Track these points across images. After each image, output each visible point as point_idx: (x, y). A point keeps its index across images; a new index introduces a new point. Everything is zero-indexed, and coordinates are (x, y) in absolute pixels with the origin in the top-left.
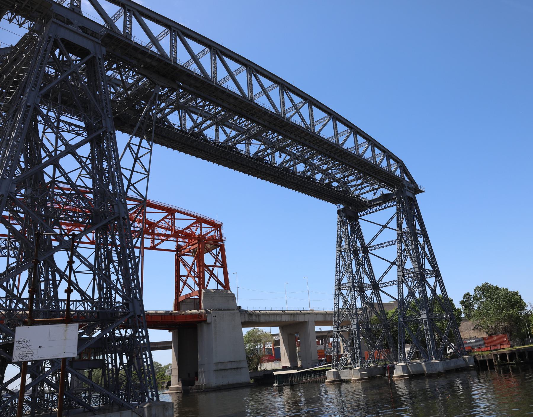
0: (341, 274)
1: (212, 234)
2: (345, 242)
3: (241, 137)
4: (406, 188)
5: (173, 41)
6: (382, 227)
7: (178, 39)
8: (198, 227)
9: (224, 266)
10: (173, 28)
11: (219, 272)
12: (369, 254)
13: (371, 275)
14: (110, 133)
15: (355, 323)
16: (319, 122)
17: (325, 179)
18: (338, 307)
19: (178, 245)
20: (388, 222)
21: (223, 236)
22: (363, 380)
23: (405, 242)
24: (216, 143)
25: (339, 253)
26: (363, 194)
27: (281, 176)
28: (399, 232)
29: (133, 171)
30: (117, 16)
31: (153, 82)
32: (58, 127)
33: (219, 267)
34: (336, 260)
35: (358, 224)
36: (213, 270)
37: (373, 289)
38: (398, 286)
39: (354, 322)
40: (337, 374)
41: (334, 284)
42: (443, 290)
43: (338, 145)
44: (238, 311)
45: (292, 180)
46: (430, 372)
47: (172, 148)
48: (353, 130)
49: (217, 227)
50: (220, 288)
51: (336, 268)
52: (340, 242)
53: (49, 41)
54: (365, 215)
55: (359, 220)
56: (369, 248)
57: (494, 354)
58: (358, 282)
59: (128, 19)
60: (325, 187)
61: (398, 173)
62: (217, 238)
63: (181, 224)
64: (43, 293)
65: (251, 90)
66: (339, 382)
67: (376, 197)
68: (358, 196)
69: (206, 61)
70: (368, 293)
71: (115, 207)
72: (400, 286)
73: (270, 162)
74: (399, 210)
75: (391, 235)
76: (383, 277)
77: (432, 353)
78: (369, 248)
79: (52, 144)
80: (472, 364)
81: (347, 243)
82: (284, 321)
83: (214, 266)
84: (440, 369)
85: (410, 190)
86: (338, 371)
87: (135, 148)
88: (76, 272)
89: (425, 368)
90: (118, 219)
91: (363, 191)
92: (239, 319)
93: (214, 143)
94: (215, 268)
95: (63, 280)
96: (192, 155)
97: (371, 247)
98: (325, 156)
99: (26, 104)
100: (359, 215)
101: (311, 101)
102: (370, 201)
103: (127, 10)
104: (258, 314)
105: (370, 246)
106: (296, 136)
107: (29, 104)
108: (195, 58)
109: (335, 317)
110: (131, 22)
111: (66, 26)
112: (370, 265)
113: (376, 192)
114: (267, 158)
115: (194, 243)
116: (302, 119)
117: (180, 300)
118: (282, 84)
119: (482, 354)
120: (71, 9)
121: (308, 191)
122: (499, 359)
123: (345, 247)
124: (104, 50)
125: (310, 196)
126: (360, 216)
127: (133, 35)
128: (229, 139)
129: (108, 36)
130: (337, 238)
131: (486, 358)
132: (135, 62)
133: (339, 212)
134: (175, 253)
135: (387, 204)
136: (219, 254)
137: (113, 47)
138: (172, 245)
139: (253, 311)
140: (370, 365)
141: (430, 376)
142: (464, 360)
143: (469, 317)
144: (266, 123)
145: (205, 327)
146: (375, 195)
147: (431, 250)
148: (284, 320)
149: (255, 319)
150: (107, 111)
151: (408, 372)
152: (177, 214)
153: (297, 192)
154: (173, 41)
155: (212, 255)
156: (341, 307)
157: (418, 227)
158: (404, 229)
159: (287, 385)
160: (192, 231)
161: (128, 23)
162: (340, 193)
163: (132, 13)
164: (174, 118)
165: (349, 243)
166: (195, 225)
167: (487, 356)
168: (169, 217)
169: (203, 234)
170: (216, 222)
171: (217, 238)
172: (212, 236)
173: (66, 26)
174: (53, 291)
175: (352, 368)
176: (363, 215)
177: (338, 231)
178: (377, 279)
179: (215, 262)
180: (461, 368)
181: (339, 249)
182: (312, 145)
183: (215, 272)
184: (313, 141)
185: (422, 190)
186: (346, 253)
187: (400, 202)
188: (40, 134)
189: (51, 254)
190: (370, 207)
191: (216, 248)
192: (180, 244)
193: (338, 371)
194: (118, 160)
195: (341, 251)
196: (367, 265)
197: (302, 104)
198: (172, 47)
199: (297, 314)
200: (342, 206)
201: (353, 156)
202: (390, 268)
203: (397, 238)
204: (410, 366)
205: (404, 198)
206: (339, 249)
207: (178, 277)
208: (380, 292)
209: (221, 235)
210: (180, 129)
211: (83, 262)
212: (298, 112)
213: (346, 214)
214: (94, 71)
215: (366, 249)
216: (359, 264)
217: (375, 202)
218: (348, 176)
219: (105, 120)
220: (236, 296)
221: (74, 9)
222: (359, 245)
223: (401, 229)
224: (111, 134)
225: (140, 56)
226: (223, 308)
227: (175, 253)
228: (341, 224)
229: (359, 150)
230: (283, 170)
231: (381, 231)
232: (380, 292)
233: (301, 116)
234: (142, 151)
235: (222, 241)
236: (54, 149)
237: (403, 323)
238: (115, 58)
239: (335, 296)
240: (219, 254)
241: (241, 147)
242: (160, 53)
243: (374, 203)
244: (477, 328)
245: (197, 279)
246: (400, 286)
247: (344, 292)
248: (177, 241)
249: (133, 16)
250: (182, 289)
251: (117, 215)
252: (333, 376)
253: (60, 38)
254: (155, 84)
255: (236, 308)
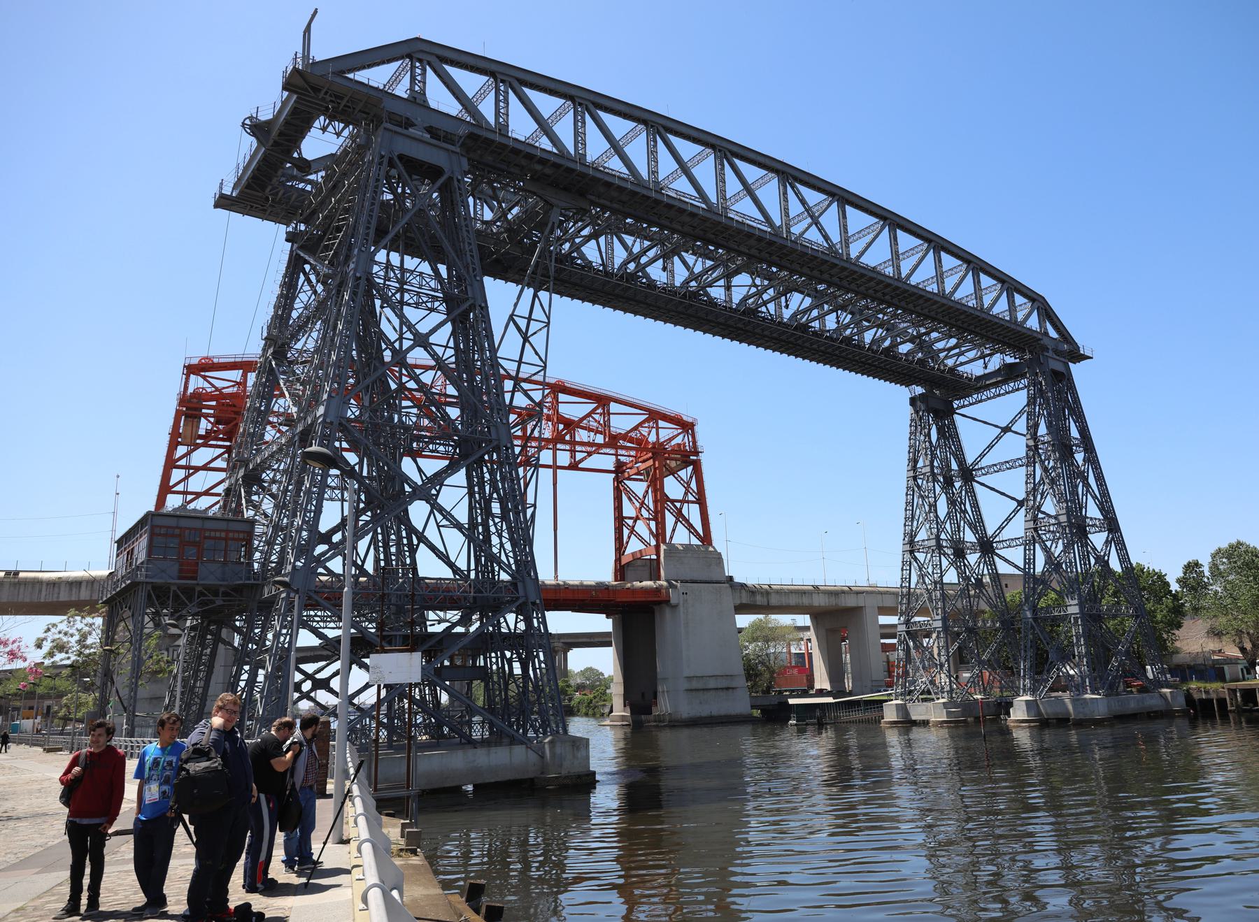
0: (915, 523)
1: (678, 440)
2: (924, 462)
3: (711, 275)
4: (1050, 354)
5: (580, 124)
6: (1000, 430)
7: (588, 118)
8: (653, 427)
9: (701, 501)
10: (578, 100)
11: (693, 512)
12: (975, 484)
13: (977, 525)
14: (480, 306)
15: (939, 617)
16: (863, 233)
17: (884, 339)
18: (907, 585)
19: (618, 460)
20: (1013, 421)
21: (699, 444)
22: (952, 724)
23: (1042, 462)
24: (669, 290)
25: (911, 483)
26: (962, 364)
27: (792, 339)
28: (1031, 443)
29: (520, 362)
30: (482, 93)
31: (545, 201)
32: (402, 303)
33: (693, 502)
34: (907, 495)
35: (953, 422)
36: (681, 508)
37: (982, 552)
38: (1025, 550)
39: (937, 615)
40: (902, 709)
41: (902, 542)
42: (1124, 558)
43: (899, 279)
44: (727, 585)
45: (815, 346)
46: (1081, 716)
47: (589, 301)
48: (933, 244)
49: (687, 427)
50: (695, 541)
51: (906, 510)
52: (914, 461)
53: (381, 164)
54: (967, 406)
55: (956, 417)
56: (974, 473)
57: (1229, 689)
58: (952, 537)
59: (501, 98)
60: (883, 357)
61: (1033, 323)
62: (687, 448)
63: (622, 422)
64: (393, 558)
65: (721, 192)
66: (907, 724)
67: (987, 371)
68: (952, 370)
69: (637, 150)
70: (973, 558)
71: (492, 429)
72: (1029, 550)
73: (771, 315)
74: (1031, 402)
75: (1015, 446)
76: (1001, 528)
77: (1087, 680)
78: (974, 473)
79: (394, 328)
80: (1179, 704)
81: (928, 463)
82: (817, 605)
83: (683, 501)
84: (1101, 711)
85: (1058, 358)
86: (905, 704)
87: (522, 324)
88: (443, 526)
89: (1070, 707)
90: (497, 449)
91: (962, 359)
92: (729, 600)
93: (664, 288)
94: (686, 505)
95: (422, 545)
96: (625, 311)
97: (979, 469)
98: (873, 301)
99: (354, 274)
100: (955, 406)
101: (843, 198)
102: (979, 378)
103: (499, 80)
104: (767, 592)
105: (976, 467)
106: (812, 269)
107: (358, 275)
108: (617, 147)
109: (901, 604)
110: (506, 101)
111: (405, 132)
112: (975, 506)
113: (989, 361)
114: (763, 309)
115: (645, 457)
116: (824, 237)
117: (622, 564)
118: (783, 173)
119: (1205, 688)
120: (412, 99)
121: (848, 363)
122: (1239, 699)
123: (923, 471)
124: (465, 162)
125: (853, 373)
126: (957, 409)
127: (510, 129)
128: (693, 277)
129: (472, 136)
130: (909, 452)
131: (1214, 696)
132: (516, 171)
133: (913, 401)
134: (613, 475)
135: (1012, 384)
136: (691, 477)
137: (479, 152)
138: (608, 462)
140: (975, 697)
141: (1080, 724)
142: (1163, 696)
143: (1196, 610)
144: (754, 252)
145: (668, 611)
146: (986, 367)
147: (1100, 478)
148: (816, 603)
149: (760, 600)
150: (474, 270)
151: (1039, 713)
152: (612, 405)
153: (828, 366)
154: (580, 124)
155: (679, 479)
156: (913, 586)
157: (1075, 433)
158: (1042, 436)
159: (813, 724)
160: (641, 434)
161: (502, 104)
162: (914, 366)
163: (508, 84)
164: (591, 252)
165: (932, 462)
166: (646, 425)
167: (1216, 691)
168: (600, 411)
169: (661, 440)
170: (685, 418)
171: (687, 448)
172: (679, 445)
173: (405, 132)
174: (410, 556)
175: (933, 700)
176: (964, 406)
177: (910, 439)
178: (990, 532)
179: (686, 494)
180: (1155, 712)
181: (911, 473)
182: (845, 283)
183: (685, 512)
184: (847, 277)
185: (1088, 353)
186: (925, 482)
187: (1035, 383)
188: (378, 309)
189: (404, 506)
190: (978, 390)
191: (686, 467)
192: (622, 459)
193: (905, 704)
194: (494, 350)
195: (915, 478)
196: (970, 505)
197: (827, 203)
198: (579, 136)
199: (843, 592)
200: (919, 390)
201: (930, 299)
202: (1016, 511)
203: (1027, 454)
204: (1042, 703)
205: (1043, 373)
206: (911, 473)
207: (620, 519)
208: (996, 559)
209: (694, 442)
210: (601, 268)
211: (449, 513)
212: (816, 222)
213: (927, 406)
214: (452, 201)
215: (968, 474)
216: (952, 502)
217: (989, 380)
218: (927, 334)
219: (471, 285)
220: (724, 557)
221: (415, 98)
222: (954, 466)
223: (1034, 436)
224: (482, 308)
225: (524, 162)
226: (696, 576)
227: (613, 475)
228: (918, 426)
229: (946, 285)
230: (796, 328)
231: (998, 438)
232: (996, 559)
233: (821, 230)
234: (534, 326)
235: (697, 453)
236: (398, 336)
237: (1031, 620)
238: (484, 170)
239: (904, 565)
240: (691, 477)
241: (717, 293)
242: (557, 150)
243: (988, 382)
244: (1216, 633)
245: (653, 524)
246: (1029, 550)
247: (920, 556)
248: (616, 455)
249: (510, 91)
250: (627, 543)
251: (495, 443)
252: (895, 713)
253: (396, 154)
254: (552, 206)
255: (724, 579)
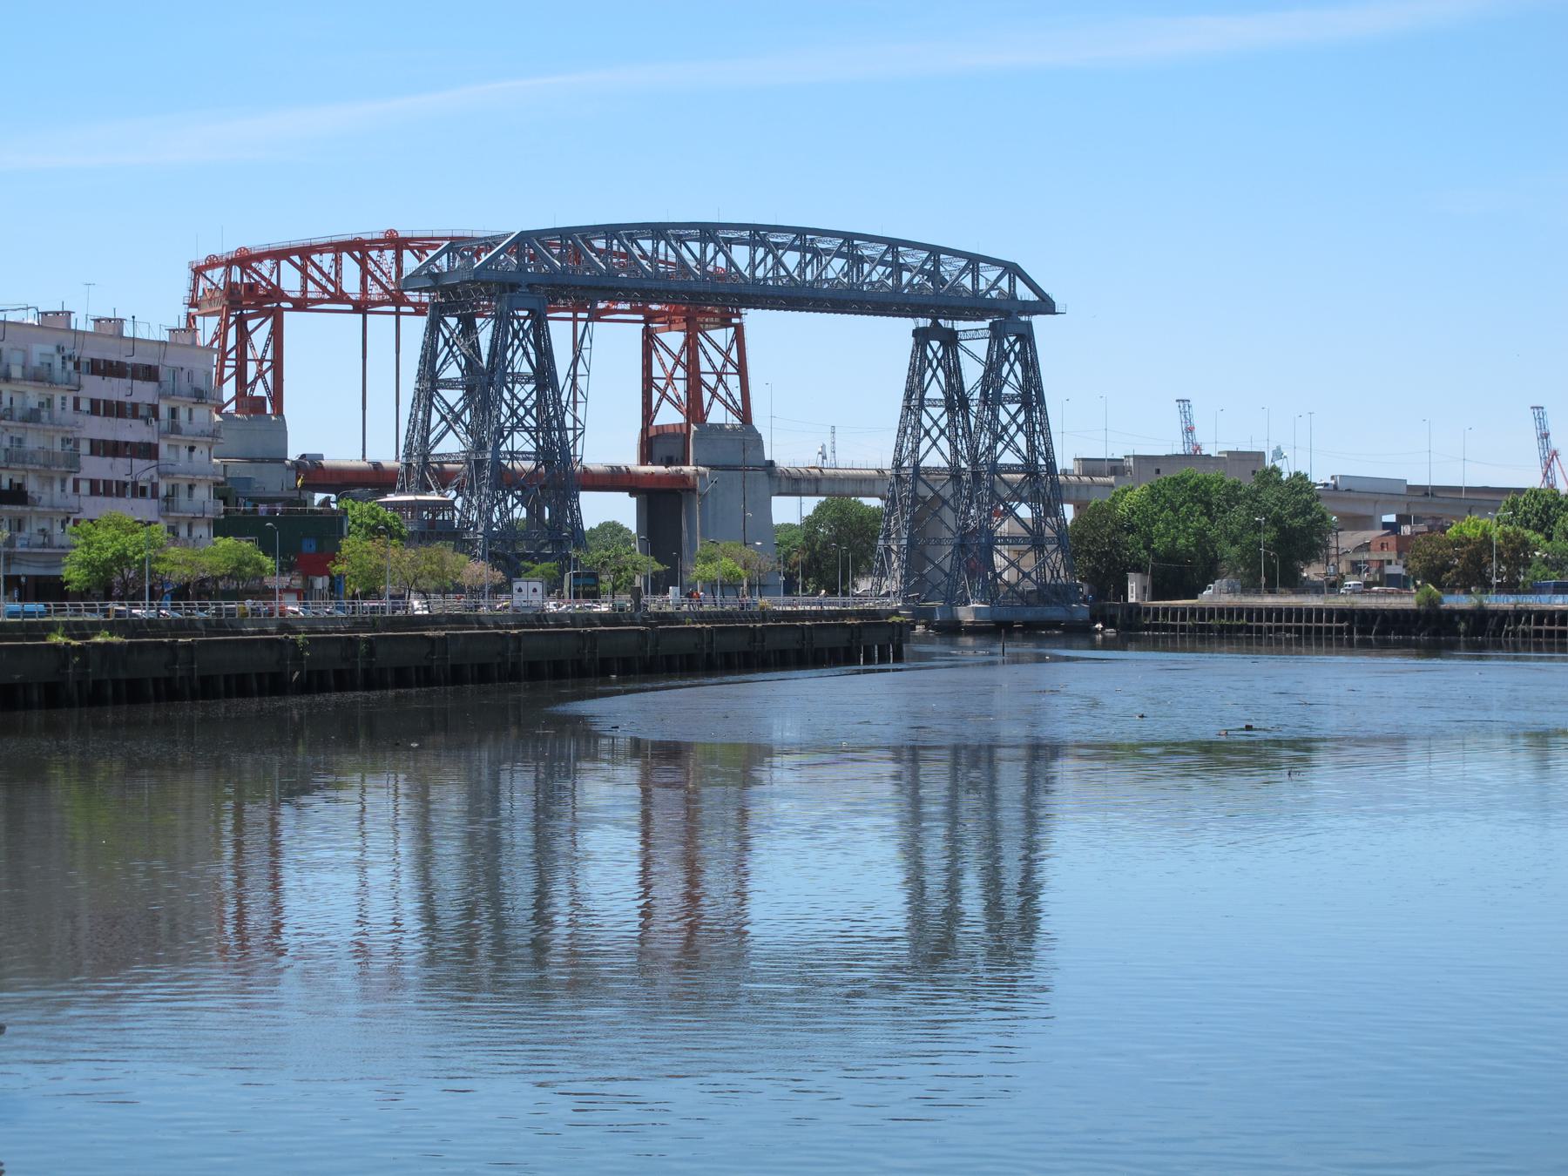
75: (977, 395)
117: (650, 435)
134: (643, 325)
139: (803, 470)
200: (925, 322)
207: (648, 381)
227: (643, 325)
255: (764, 464)
